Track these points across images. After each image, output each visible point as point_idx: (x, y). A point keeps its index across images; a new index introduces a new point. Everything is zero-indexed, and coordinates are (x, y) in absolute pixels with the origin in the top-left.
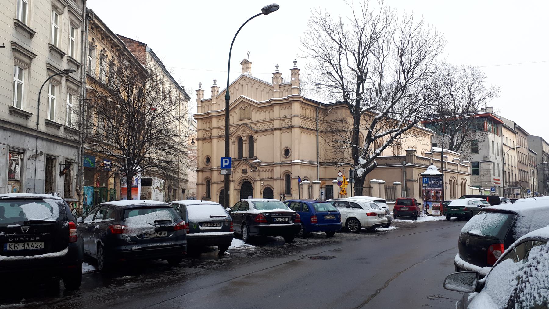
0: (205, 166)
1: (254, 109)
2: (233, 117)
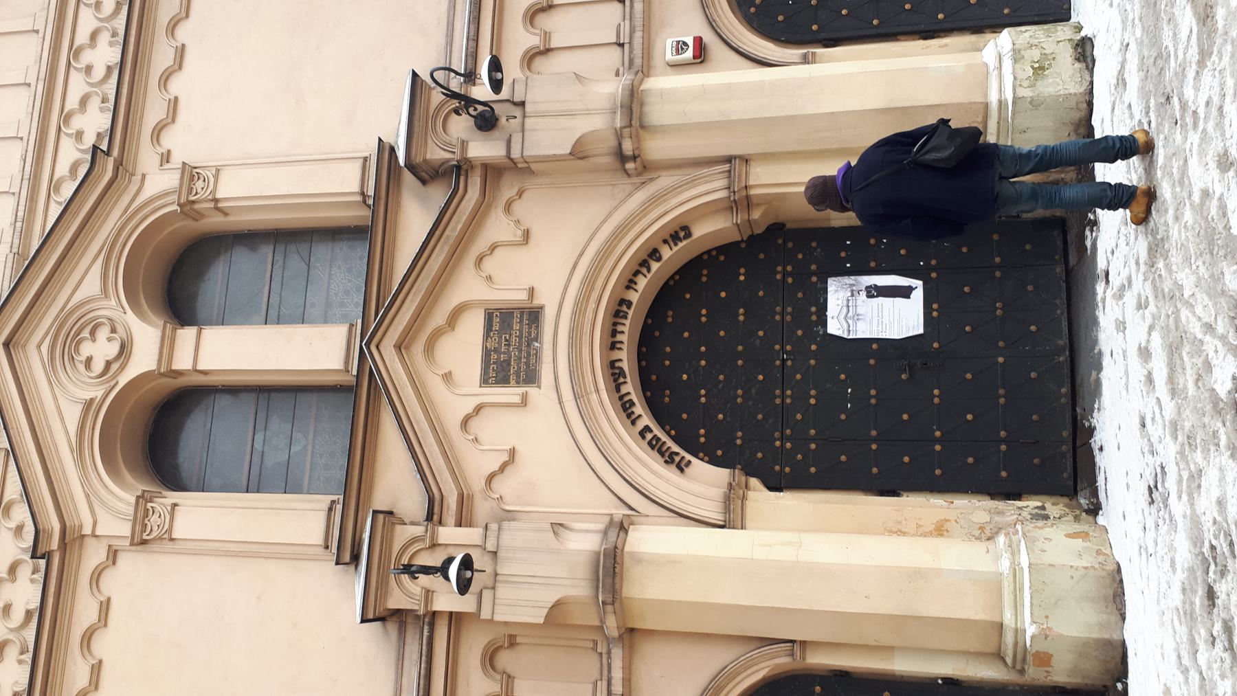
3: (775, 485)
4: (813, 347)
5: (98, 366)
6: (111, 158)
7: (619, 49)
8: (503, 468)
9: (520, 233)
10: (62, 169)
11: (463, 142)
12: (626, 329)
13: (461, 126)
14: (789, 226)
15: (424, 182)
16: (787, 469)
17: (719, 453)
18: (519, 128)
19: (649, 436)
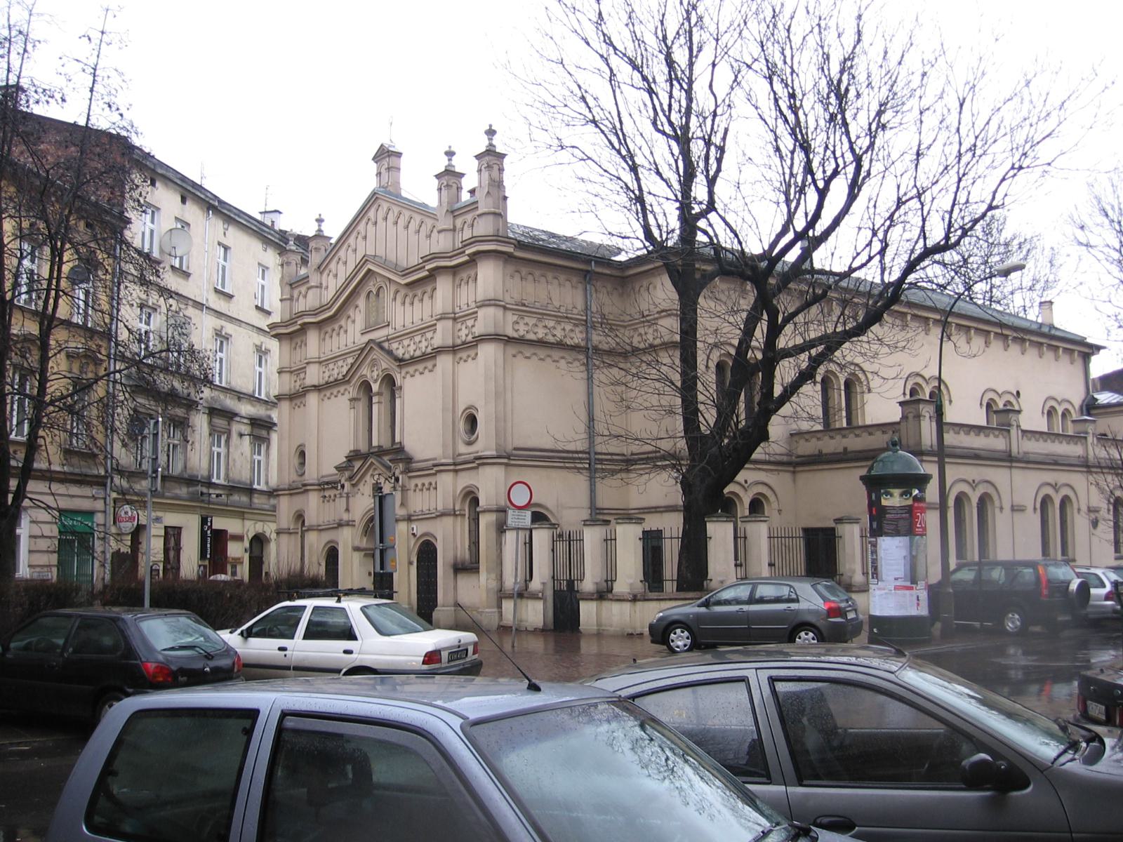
1: (397, 292)
2: (354, 322)
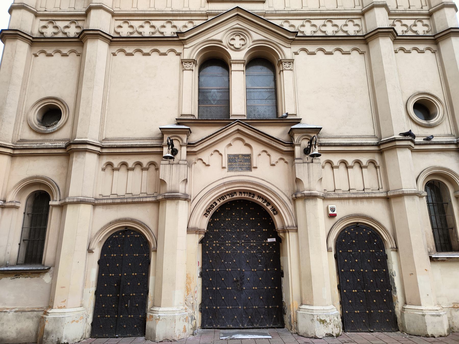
0: (28, 135)
3: (202, 242)
4: (243, 252)
5: (232, 42)
6: (296, 38)
7: (333, 190)
8: (204, 163)
9: (274, 163)
10: (292, 22)
11: (300, 145)
12: (246, 196)
13: (305, 143)
14: (281, 244)
15: (289, 133)
16: (207, 245)
17: (212, 225)
18: (305, 161)
19: (214, 205)
